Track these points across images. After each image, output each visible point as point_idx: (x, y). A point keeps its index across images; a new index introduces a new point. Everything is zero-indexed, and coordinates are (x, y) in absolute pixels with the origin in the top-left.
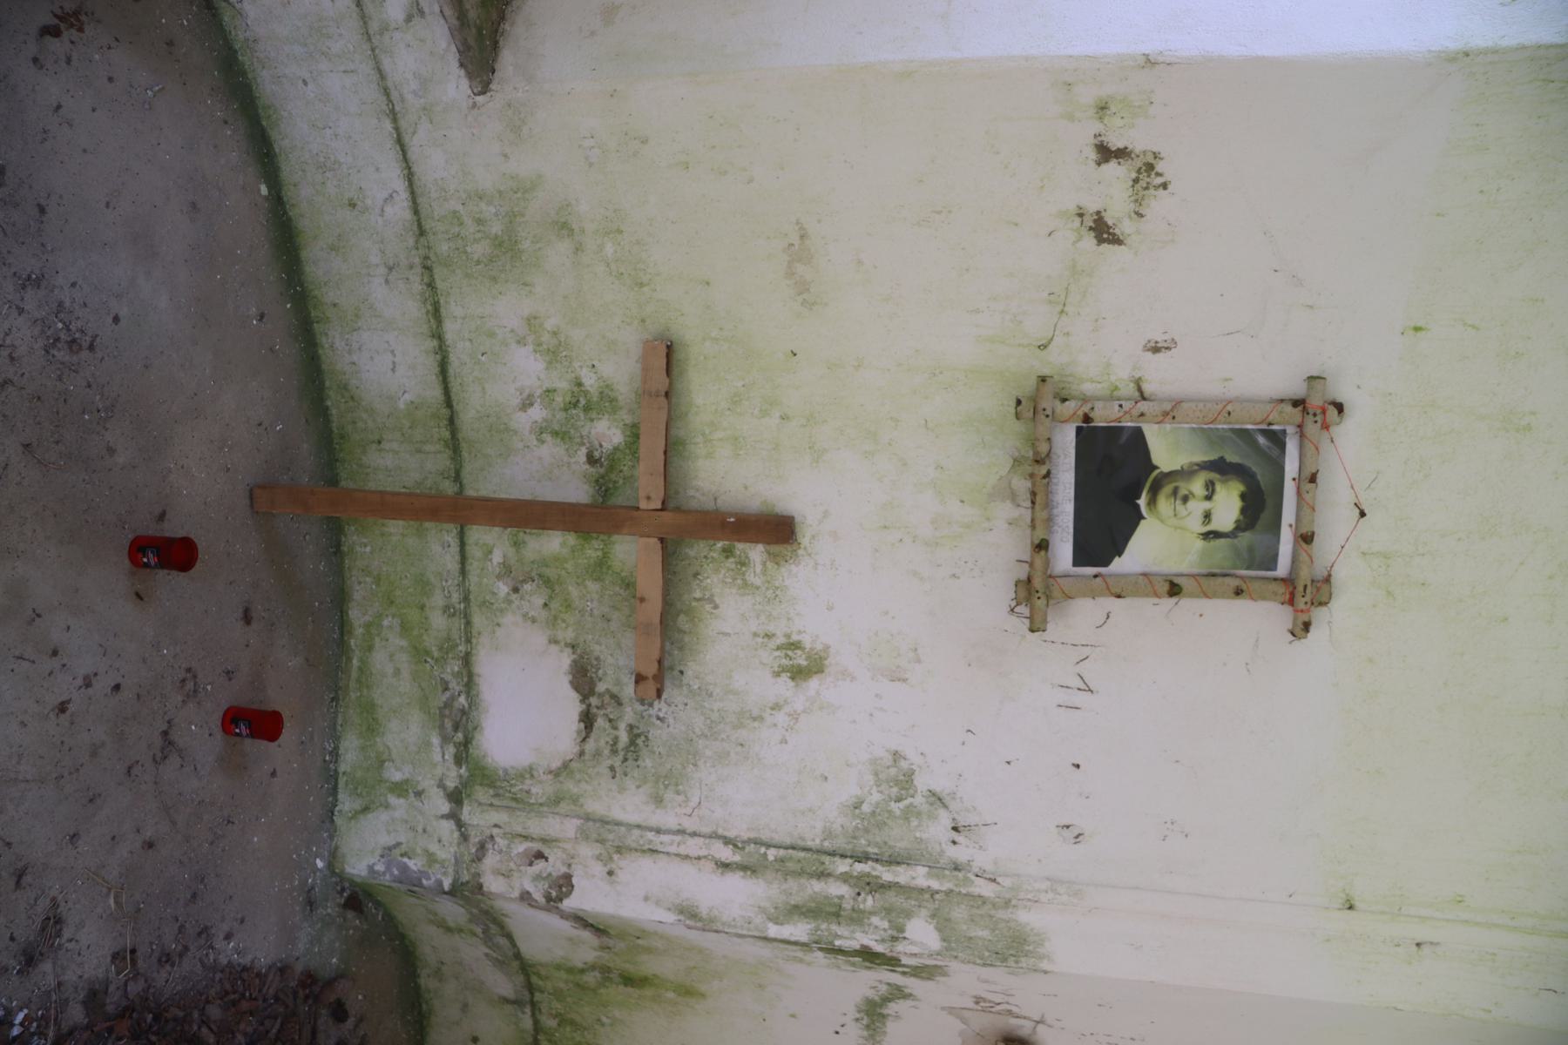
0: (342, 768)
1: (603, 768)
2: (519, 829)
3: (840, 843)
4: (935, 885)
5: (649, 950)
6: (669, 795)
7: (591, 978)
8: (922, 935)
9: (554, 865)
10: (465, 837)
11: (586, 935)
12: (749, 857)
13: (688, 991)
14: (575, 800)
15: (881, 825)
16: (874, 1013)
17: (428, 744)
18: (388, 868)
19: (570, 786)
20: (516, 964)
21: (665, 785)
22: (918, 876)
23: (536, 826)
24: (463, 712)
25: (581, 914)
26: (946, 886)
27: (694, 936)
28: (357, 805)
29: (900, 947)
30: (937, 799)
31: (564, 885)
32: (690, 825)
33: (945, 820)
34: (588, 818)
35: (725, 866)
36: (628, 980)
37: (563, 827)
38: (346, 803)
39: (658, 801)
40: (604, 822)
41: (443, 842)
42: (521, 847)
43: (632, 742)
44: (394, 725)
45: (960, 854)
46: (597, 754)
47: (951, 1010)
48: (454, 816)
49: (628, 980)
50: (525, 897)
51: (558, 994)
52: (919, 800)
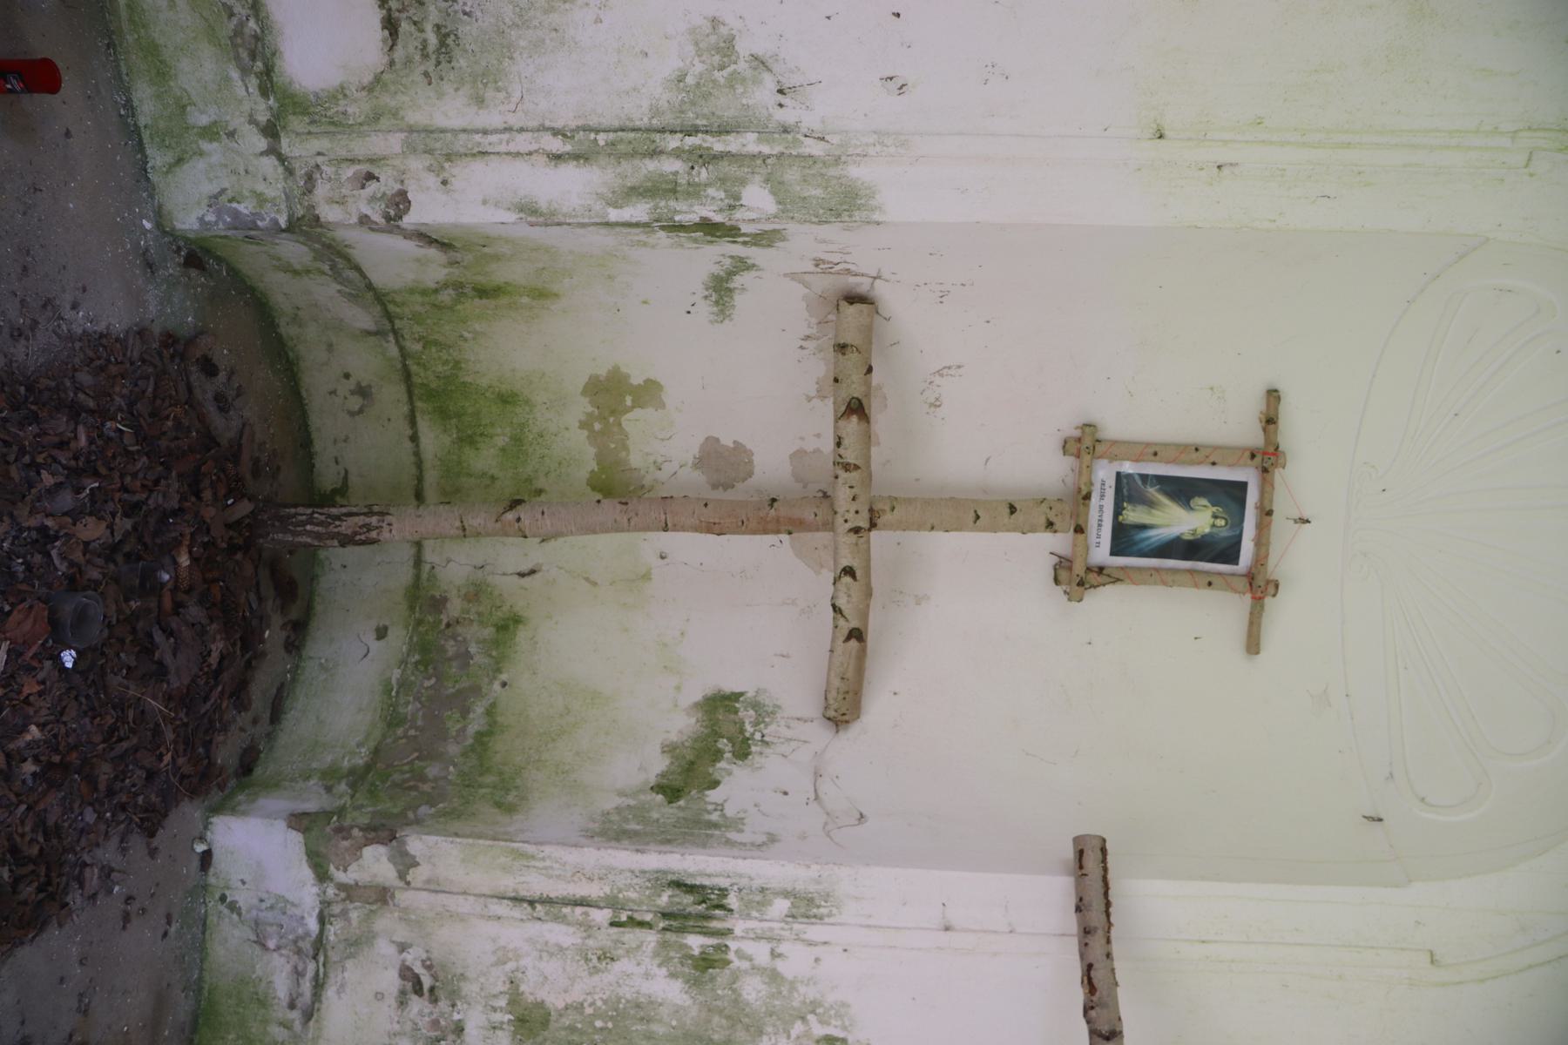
0: (142, 121)
1: (417, 76)
2: (343, 153)
3: (669, 119)
4: (766, 150)
5: (497, 258)
6: (489, 93)
7: (446, 297)
8: (758, 200)
9: (387, 184)
10: (290, 172)
11: (433, 252)
12: (579, 146)
13: (541, 295)
14: (395, 114)
15: (707, 96)
16: (721, 289)
17: (228, 79)
18: (219, 213)
19: (386, 100)
20: (370, 295)
21: (483, 84)
22: (749, 143)
23: (360, 147)
24: (256, 38)
25: (423, 229)
26: (777, 150)
27: (539, 234)
28: (170, 157)
29: (738, 215)
30: (760, 63)
31: (401, 202)
32: (515, 121)
33: (770, 84)
34: (411, 130)
35: (557, 158)
36: (482, 292)
37: (387, 143)
38: (158, 158)
39: (480, 101)
40: (428, 131)
41: (268, 179)
42: (349, 171)
43: (442, 43)
44: (185, 65)
45: (788, 116)
46: (408, 61)
47: (793, 276)
48: (273, 151)
49: (482, 292)
50: (364, 220)
51: (417, 318)
52: (742, 66)
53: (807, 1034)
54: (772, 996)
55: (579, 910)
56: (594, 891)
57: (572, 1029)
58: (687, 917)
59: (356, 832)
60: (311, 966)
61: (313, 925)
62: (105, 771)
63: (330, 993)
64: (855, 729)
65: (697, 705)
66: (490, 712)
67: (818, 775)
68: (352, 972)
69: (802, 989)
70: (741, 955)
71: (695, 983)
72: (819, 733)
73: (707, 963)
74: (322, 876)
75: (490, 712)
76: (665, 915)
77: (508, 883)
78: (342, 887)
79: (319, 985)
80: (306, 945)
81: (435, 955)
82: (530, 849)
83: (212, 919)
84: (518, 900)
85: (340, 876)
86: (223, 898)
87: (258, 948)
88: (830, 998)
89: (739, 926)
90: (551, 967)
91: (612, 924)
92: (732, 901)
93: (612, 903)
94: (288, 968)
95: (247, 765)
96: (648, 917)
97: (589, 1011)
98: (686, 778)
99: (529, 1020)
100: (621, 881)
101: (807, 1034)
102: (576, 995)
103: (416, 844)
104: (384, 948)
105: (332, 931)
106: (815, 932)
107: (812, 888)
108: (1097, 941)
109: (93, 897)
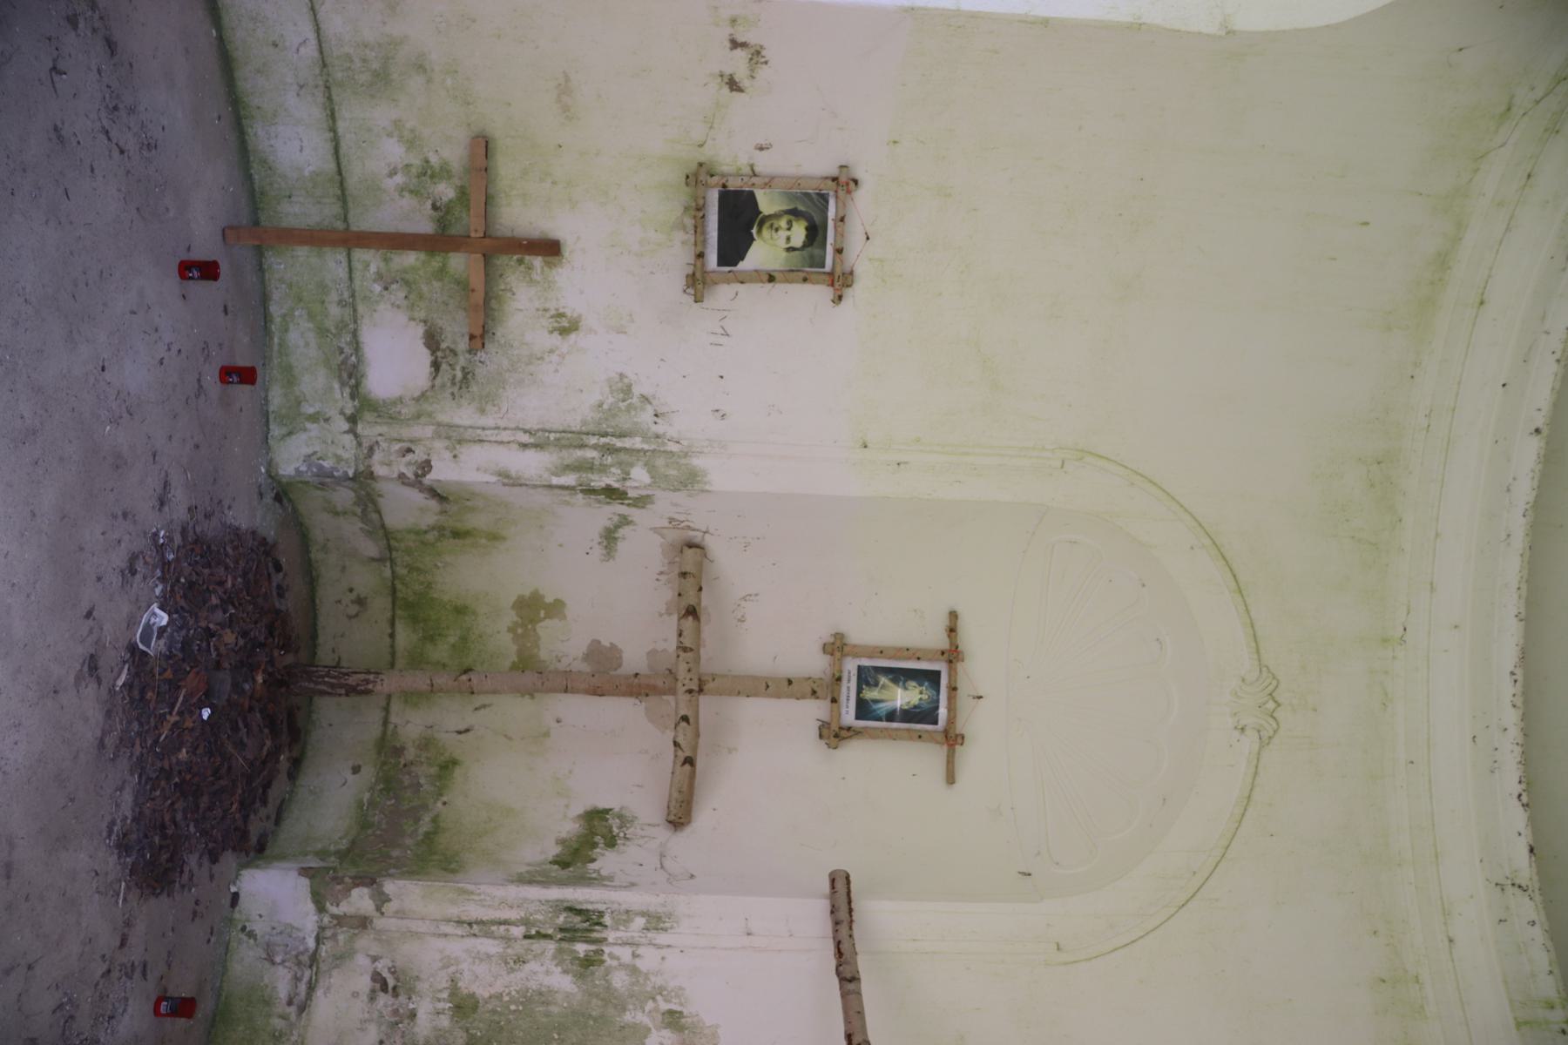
0: (271, 409)
1: (447, 395)
2: (395, 435)
3: (591, 428)
4: (646, 447)
5: (472, 510)
6: (489, 407)
7: (430, 537)
8: (640, 475)
9: (419, 455)
10: (360, 444)
11: (433, 504)
12: (538, 441)
13: (495, 537)
14: (430, 415)
15: (614, 416)
16: (610, 538)
17: (331, 388)
18: (309, 467)
19: (427, 407)
20: (381, 532)
21: (485, 402)
22: (636, 443)
23: (406, 432)
24: (354, 366)
25: (435, 486)
26: (653, 447)
27: (505, 492)
28: (284, 431)
29: (628, 483)
30: (645, 399)
31: (426, 466)
32: (502, 424)
33: (650, 410)
34: (439, 424)
35: (524, 446)
36: (457, 534)
37: (423, 431)
38: (276, 430)
39: (482, 411)
40: (450, 426)
41: (346, 448)
42: (397, 447)
43: (465, 377)
44: (306, 378)
45: (660, 429)
46: (443, 386)
47: (655, 530)
48: (352, 431)
49: (457, 534)
50: (402, 476)
51: (409, 552)
52: (635, 400)
53: (656, 1009)
54: (633, 984)
55: (502, 928)
56: (513, 915)
57: (494, 1012)
58: (576, 931)
59: (347, 880)
60: (307, 973)
61: (311, 943)
62: (204, 801)
63: (319, 993)
64: (688, 830)
65: (580, 816)
66: (435, 820)
67: (662, 856)
68: (336, 978)
69: (653, 979)
70: (612, 956)
71: (580, 977)
72: (663, 834)
73: (589, 962)
74: (321, 909)
75: (435, 820)
76: (562, 930)
77: (453, 911)
78: (333, 916)
79: (311, 988)
80: (305, 959)
81: (398, 964)
82: (470, 887)
83: (234, 944)
84: (460, 922)
85: (334, 910)
86: (244, 929)
87: (267, 964)
88: (672, 985)
89: (611, 936)
90: (481, 969)
91: (526, 937)
92: (607, 920)
93: (525, 922)
94: (289, 976)
95: (261, 848)
96: (550, 931)
97: (506, 999)
98: (574, 858)
99: (463, 1006)
100: (532, 908)
101: (656, 1009)
102: (498, 987)
103: (390, 887)
104: (362, 960)
105: (325, 950)
106: (662, 938)
107: (660, 910)
108: (844, 929)
109: (183, 886)
